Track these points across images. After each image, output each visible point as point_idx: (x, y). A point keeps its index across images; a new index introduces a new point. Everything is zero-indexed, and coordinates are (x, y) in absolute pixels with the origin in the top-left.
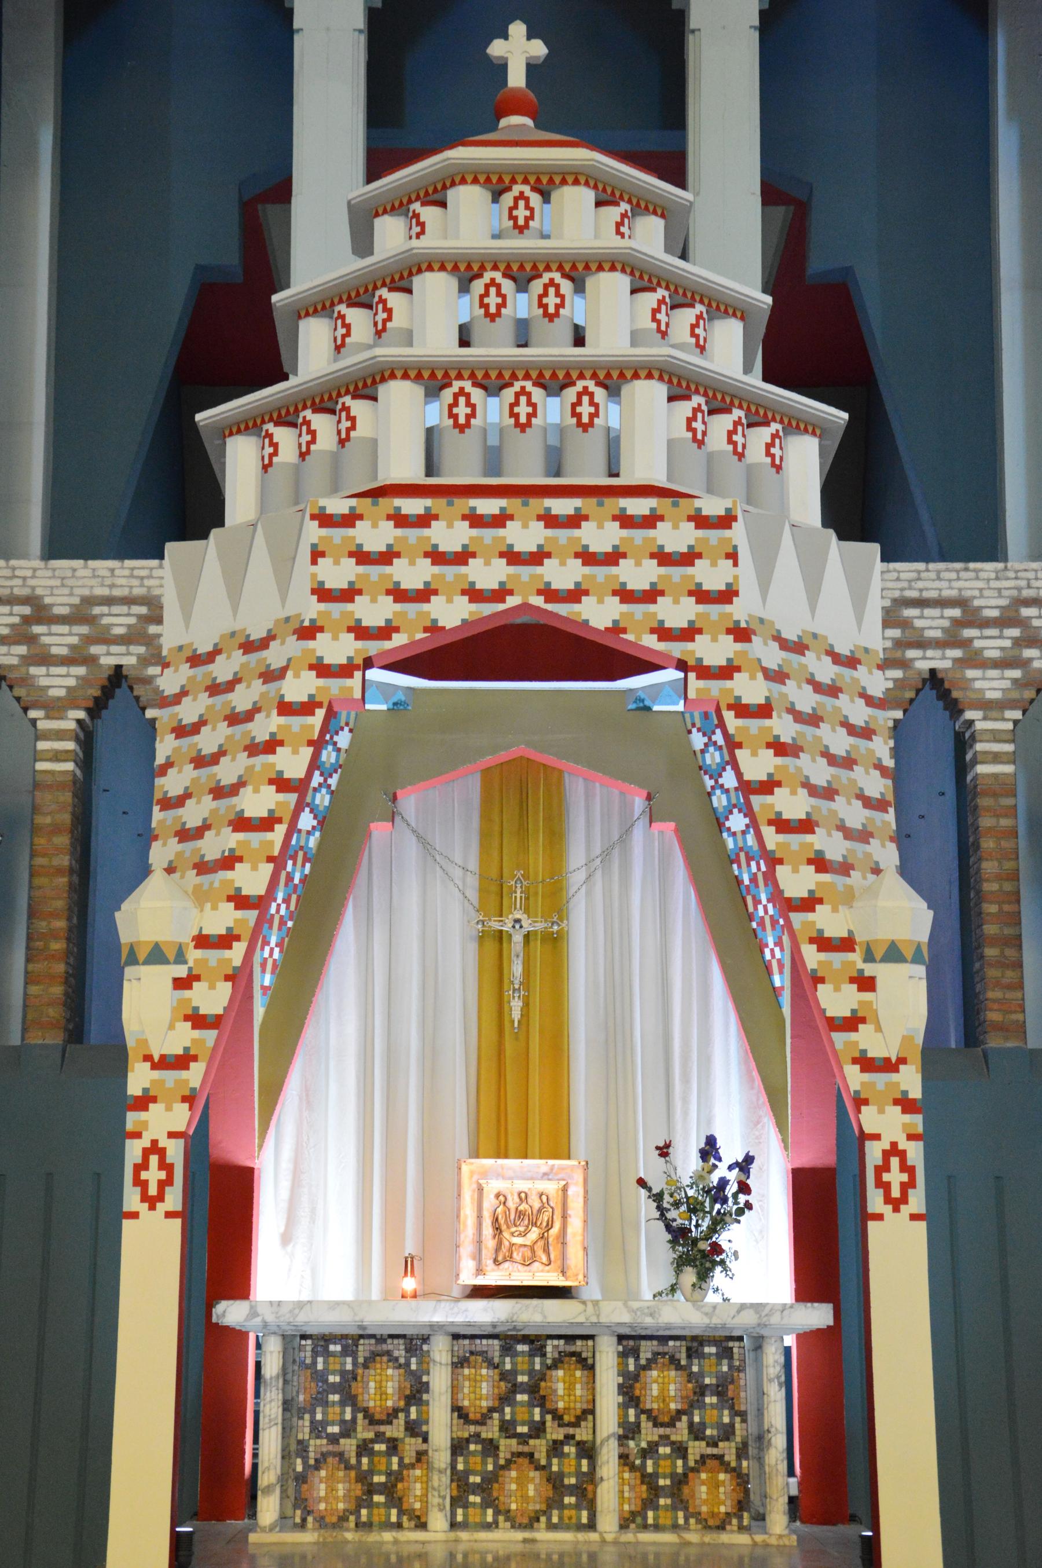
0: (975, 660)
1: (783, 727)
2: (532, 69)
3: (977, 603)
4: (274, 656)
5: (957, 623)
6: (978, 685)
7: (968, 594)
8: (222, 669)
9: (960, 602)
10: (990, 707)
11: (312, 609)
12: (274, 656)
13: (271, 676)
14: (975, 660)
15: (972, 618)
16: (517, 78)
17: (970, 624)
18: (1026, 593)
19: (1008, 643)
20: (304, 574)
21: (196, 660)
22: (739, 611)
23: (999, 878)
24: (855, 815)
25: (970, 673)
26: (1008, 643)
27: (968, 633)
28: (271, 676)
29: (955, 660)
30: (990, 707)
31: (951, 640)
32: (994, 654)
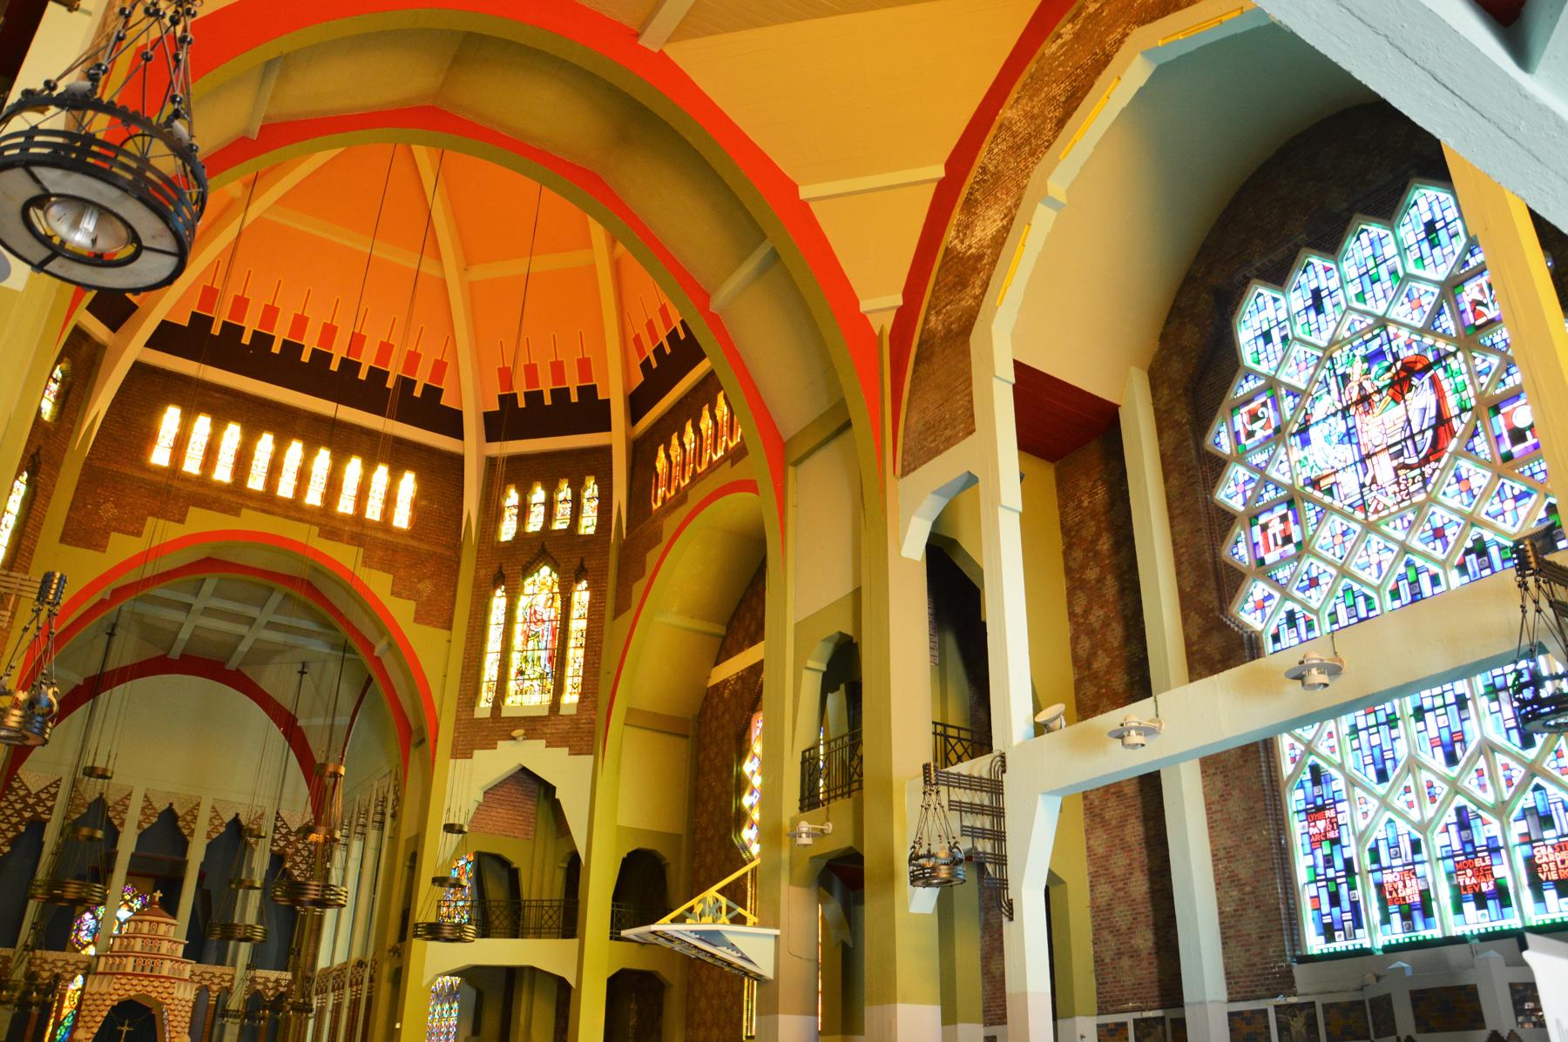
1: (176, 1013)
2: (160, 898)
4: (105, 997)
8: (95, 997)
10: (214, 992)
11: (112, 991)
12: (105, 997)
13: (104, 1000)
14: (213, 983)
15: (214, 976)
16: (157, 899)
20: (112, 985)
21: (91, 994)
22: (174, 996)
24: (183, 1024)
28: (104, 1000)
30: (214, 992)
31: (210, 979)
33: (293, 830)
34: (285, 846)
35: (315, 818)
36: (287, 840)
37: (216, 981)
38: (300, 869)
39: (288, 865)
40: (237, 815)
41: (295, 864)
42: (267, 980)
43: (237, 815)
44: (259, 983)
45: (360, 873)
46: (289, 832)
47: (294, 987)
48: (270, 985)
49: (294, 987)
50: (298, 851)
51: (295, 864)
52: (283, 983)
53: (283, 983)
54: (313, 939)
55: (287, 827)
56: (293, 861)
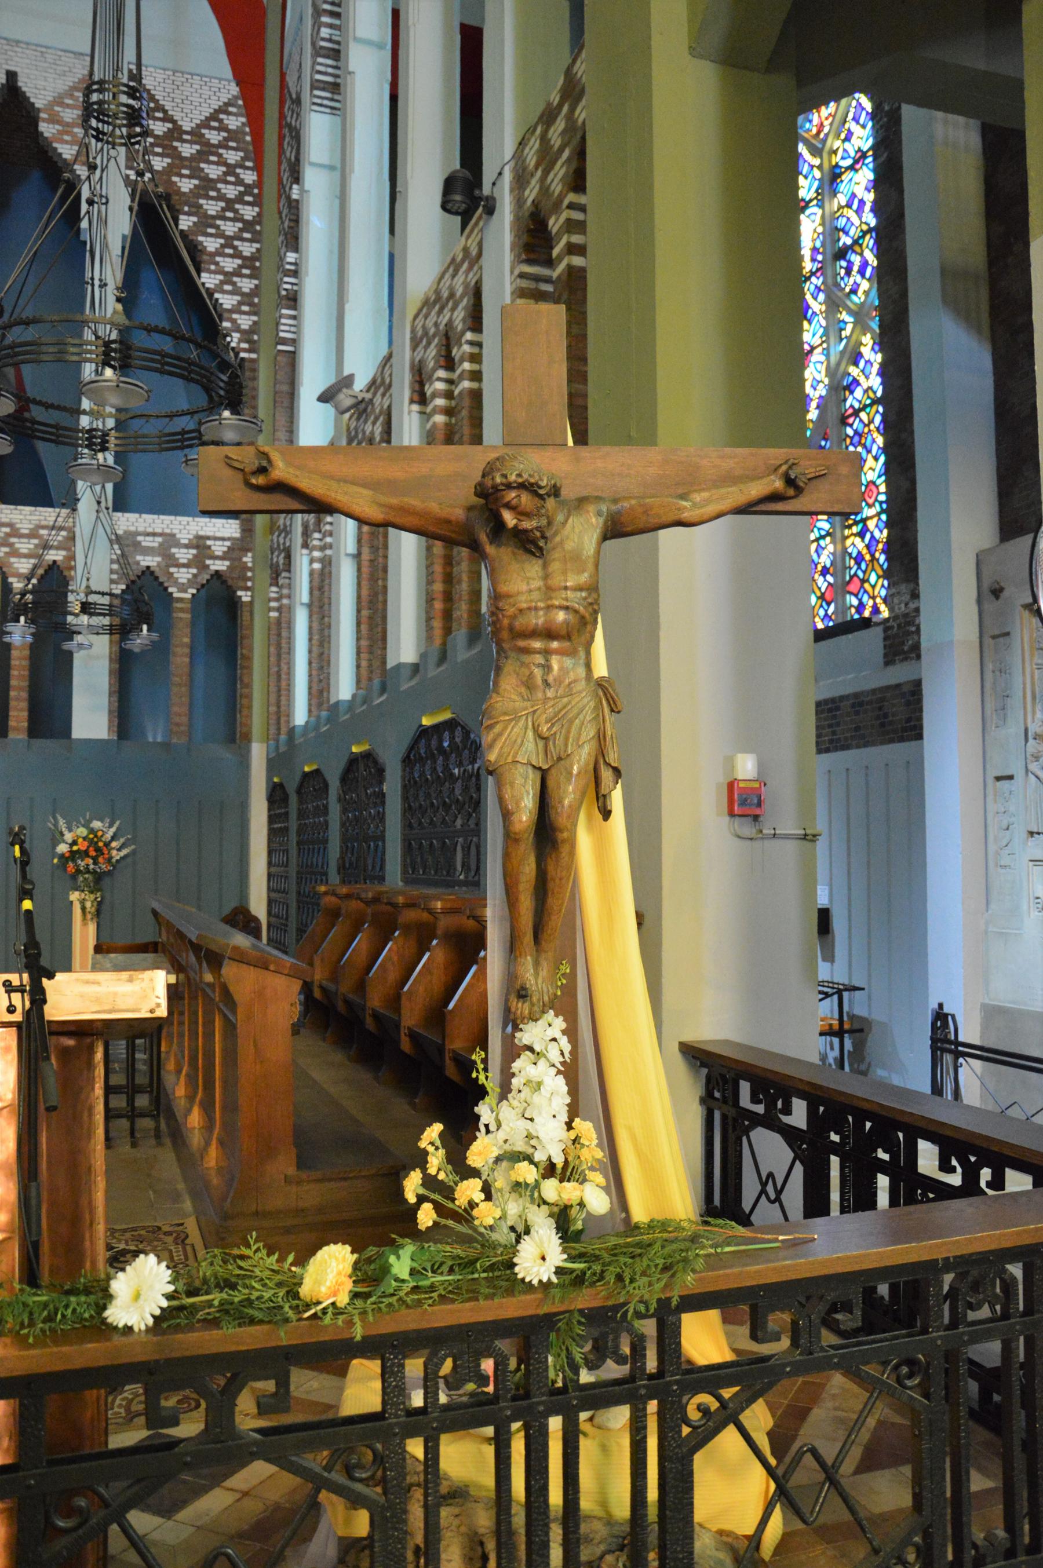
0: (15, 553)
3: (18, 526)
5: (8, 535)
6: (16, 565)
7: (14, 521)
9: (10, 525)
17: (15, 536)
18: (43, 523)
19: (32, 546)
23: (20, 658)
25: (13, 560)
26: (32, 546)
27: (13, 540)
29: (6, 553)
32: (25, 551)
33: (187, 126)
34: (169, 171)
35: (244, 94)
36: (175, 154)
37: (25, 546)
38: (220, 234)
39: (186, 222)
40: (11, 76)
41: (206, 222)
42: (170, 539)
43: (11, 76)
44: (147, 551)
45: (391, 257)
46: (176, 132)
47: (248, 559)
48: (184, 555)
49: (248, 559)
50: (207, 184)
51: (206, 222)
52: (219, 548)
53: (219, 548)
54: (282, 420)
55: (167, 118)
56: (197, 210)
